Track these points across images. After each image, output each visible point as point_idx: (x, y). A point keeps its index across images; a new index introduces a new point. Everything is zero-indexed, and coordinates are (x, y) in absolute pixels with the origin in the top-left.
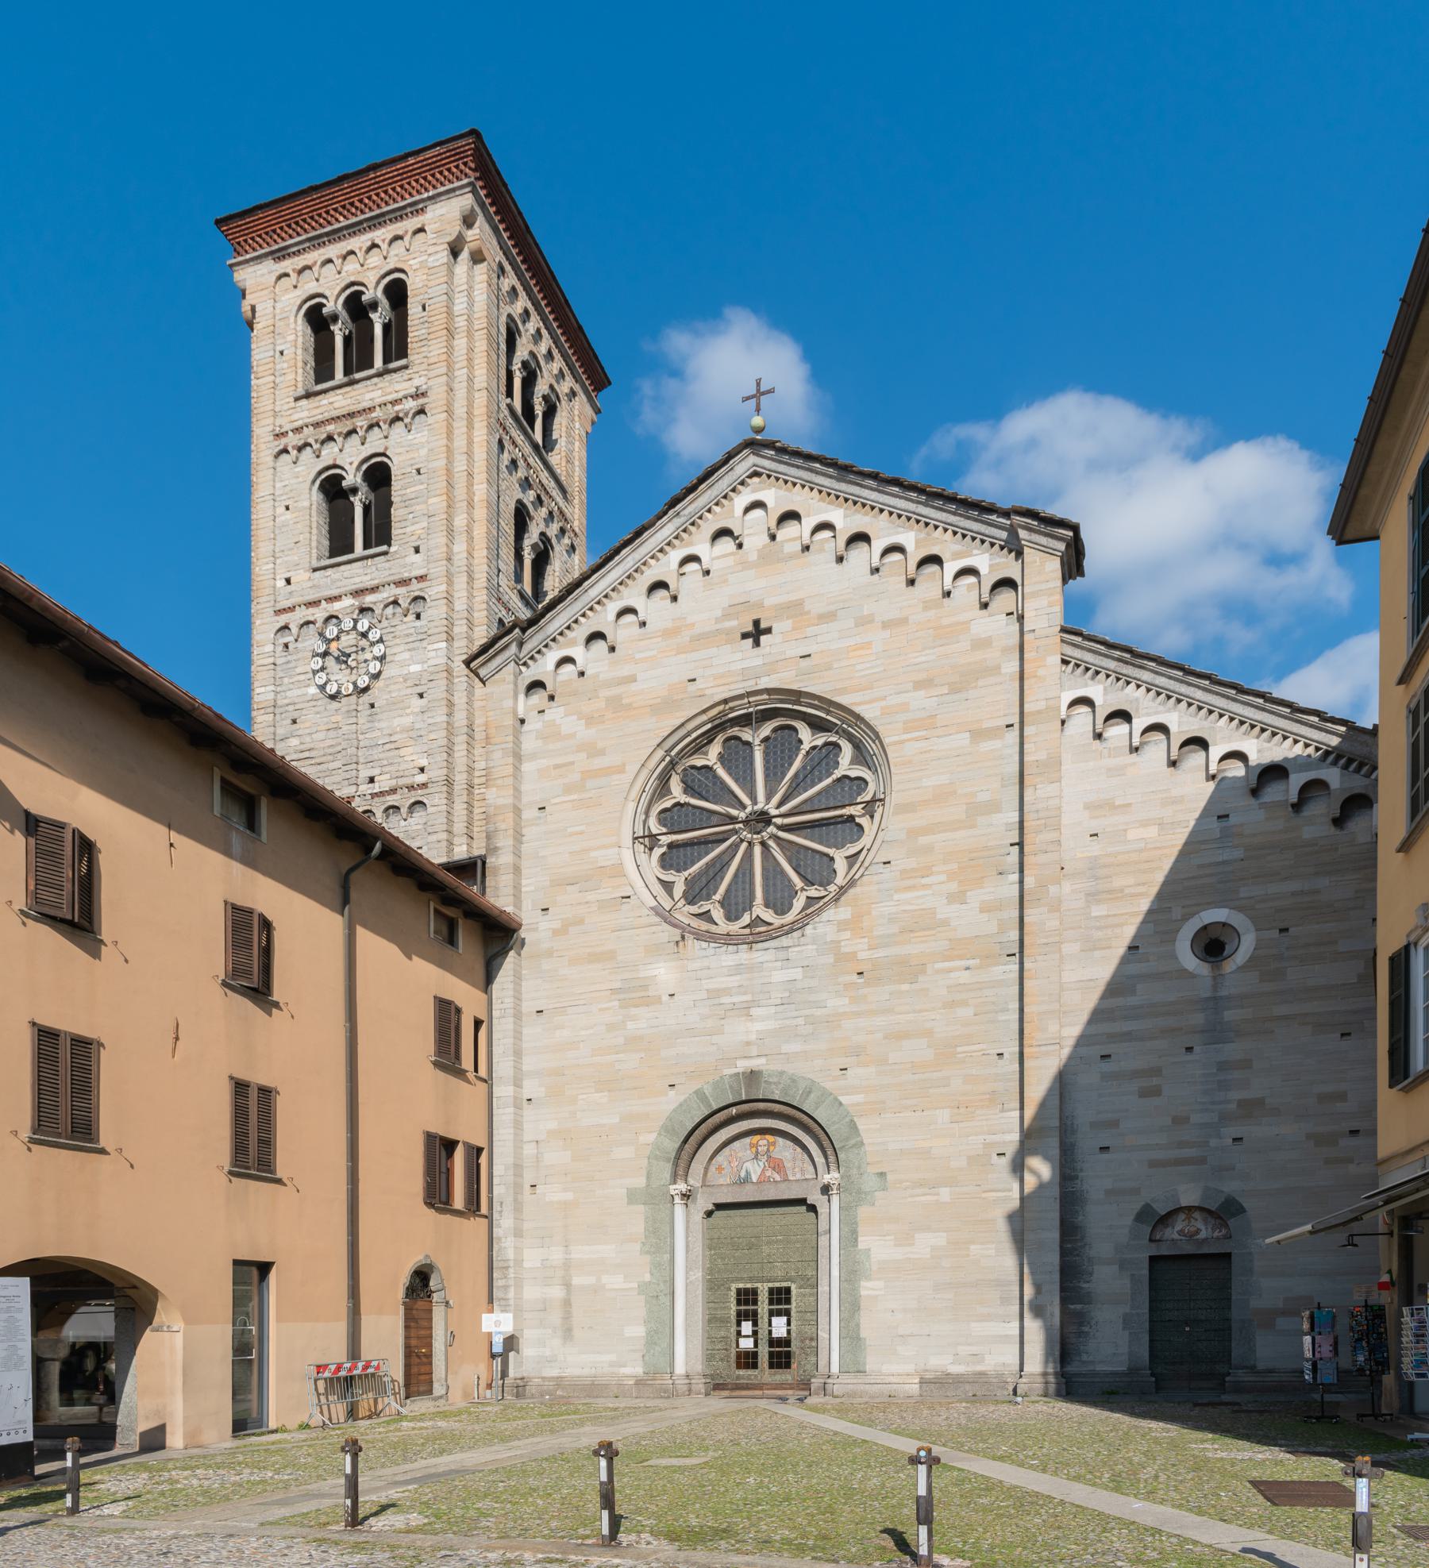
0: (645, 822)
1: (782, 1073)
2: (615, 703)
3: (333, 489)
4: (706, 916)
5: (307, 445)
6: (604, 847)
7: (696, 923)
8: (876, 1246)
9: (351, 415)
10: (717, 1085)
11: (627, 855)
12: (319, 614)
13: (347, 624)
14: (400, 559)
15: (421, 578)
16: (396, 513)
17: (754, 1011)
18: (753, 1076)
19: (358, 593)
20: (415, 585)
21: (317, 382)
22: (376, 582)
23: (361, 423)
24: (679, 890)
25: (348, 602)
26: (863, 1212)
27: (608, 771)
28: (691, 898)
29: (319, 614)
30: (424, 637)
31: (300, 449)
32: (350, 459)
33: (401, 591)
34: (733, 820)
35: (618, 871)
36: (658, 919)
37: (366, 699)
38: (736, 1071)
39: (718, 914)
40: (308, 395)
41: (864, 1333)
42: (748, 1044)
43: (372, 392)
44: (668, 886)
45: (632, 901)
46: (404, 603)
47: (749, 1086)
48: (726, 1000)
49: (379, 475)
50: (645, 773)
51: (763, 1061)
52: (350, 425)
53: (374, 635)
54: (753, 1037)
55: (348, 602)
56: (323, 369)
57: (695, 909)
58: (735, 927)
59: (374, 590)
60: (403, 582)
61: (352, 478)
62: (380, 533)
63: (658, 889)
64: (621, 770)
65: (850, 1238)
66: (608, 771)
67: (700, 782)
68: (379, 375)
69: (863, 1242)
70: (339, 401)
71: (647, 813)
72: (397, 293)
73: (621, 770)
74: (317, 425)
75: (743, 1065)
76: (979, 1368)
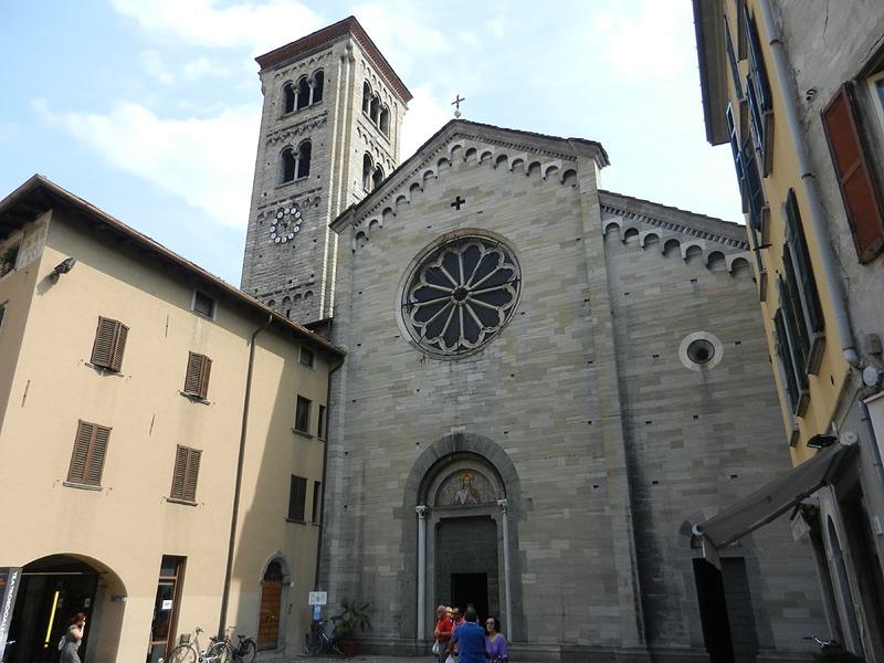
0: (408, 297)
1: (474, 435)
2: (395, 240)
3: (287, 156)
4: (436, 346)
5: (279, 138)
6: (388, 311)
7: (431, 349)
8: (531, 550)
9: (297, 125)
10: (440, 442)
11: (398, 314)
12: (276, 208)
13: (287, 211)
14: (312, 181)
15: (320, 189)
16: (312, 162)
17: (460, 399)
18: (459, 436)
19: (292, 198)
20: (316, 192)
21: (287, 112)
22: (299, 193)
23: (301, 127)
24: (423, 332)
25: (289, 201)
26: (521, 524)
27: (392, 272)
28: (429, 335)
29: (276, 208)
30: (318, 214)
31: (276, 140)
32: (295, 142)
33: (308, 195)
34: (449, 294)
35: (394, 323)
36: (411, 348)
37: (292, 244)
38: (449, 434)
39: (442, 344)
40: (282, 118)
41: (525, 613)
42: (457, 417)
43: (306, 115)
44: (418, 330)
45: (401, 339)
46: (311, 201)
47: (457, 443)
48: (445, 392)
49: (306, 147)
50: (408, 273)
51: (464, 428)
52: (296, 129)
53: (297, 215)
54: (459, 414)
55: (289, 201)
56: (289, 108)
57: (430, 342)
58: (450, 351)
59: (299, 195)
60: (313, 191)
61: (295, 149)
62: (304, 171)
63: (413, 331)
64: (397, 271)
65: (514, 544)
66: (392, 272)
67: (435, 276)
68: (310, 108)
69: (523, 545)
70: (294, 120)
71: (409, 292)
72: (320, 76)
73: (397, 271)
74: (284, 130)
75: (454, 430)
76: (596, 642)
